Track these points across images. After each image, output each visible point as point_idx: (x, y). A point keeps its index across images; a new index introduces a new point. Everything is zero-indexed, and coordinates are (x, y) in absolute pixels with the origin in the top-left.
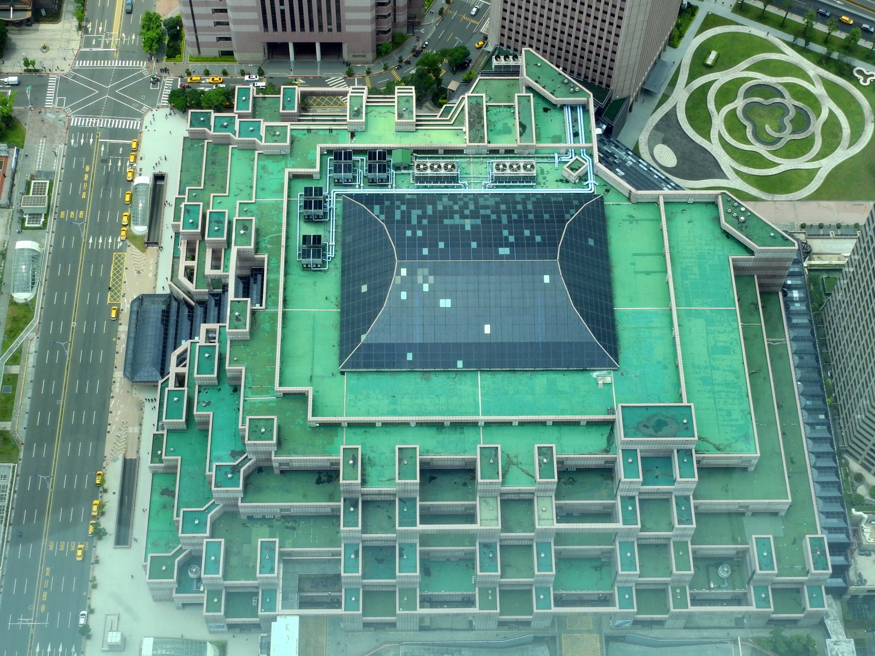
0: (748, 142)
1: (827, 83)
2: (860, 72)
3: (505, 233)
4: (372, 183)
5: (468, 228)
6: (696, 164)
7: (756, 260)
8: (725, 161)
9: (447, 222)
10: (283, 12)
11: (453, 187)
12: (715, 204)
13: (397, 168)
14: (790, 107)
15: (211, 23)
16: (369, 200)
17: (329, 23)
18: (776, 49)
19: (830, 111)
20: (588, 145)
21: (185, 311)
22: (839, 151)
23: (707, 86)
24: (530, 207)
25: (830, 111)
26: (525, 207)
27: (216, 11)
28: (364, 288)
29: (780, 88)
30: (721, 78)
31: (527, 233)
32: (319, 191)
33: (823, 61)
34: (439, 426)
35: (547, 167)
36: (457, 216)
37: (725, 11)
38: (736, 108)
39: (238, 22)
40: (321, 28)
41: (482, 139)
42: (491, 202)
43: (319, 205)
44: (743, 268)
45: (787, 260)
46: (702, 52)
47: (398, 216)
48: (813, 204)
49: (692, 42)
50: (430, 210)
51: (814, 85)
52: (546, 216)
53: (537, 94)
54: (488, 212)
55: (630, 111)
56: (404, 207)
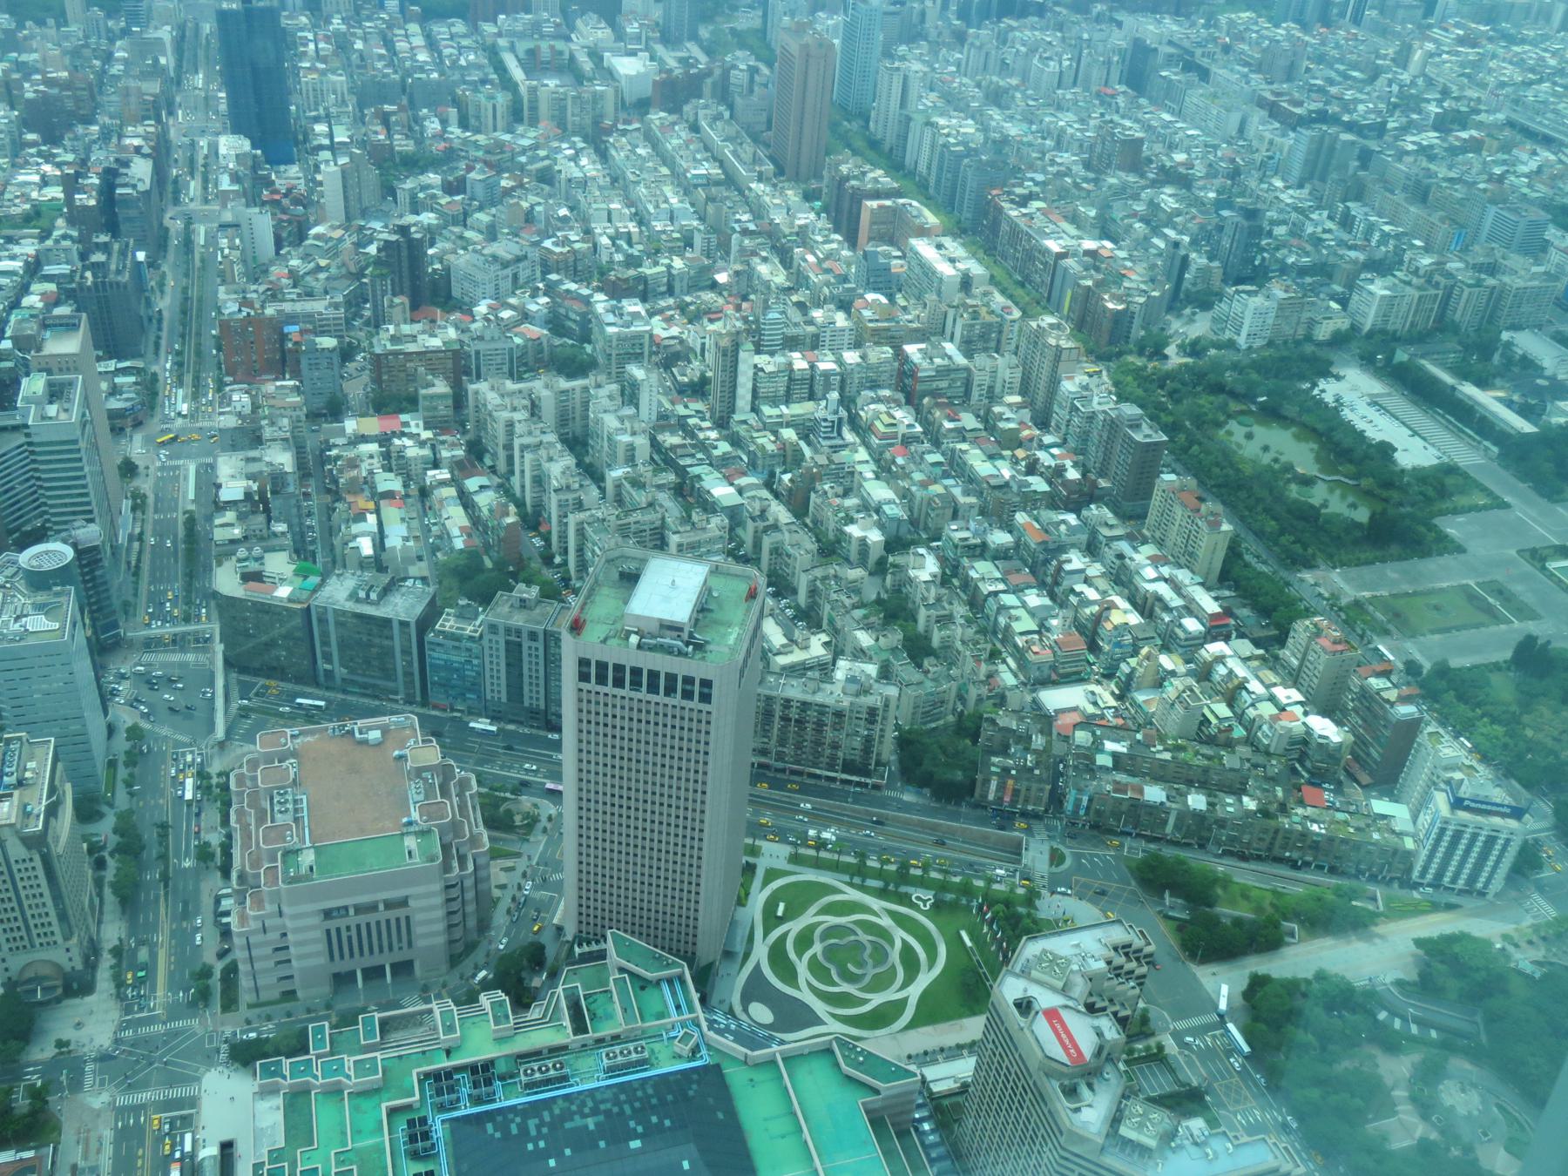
0: (834, 984)
1: (893, 915)
2: (918, 898)
3: (632, 1124)
4: (478, 1101)
5: (592, 1127)
6: (793, 1016)
8: (819, 1007)
9: (568, 1125)
10: (350, 938)
13: (502, 1078)
15: (272, 964)
16: (478, 1119)
17: (400, 940)
22: (920, 976)
23: (784, 937)
24: (650, 1091)
25: (903, 941)
30: (795, 927)
31: (654, 1119)
32: (423, 1121)
33: (882, 894)
35: (657, 1047)
36: (577, 1117)
37: (782, 864)
39: (300, 957)
40: (391, 949)
42: (609, 1094)
43: (426, 1136)
44: (875, 1110)
45: (911, 1093)
47: (514, 1130)
48: (912, 1033)
49: (759, 898)
50: (547, 1116)
52: (670, 1098)
53: (631, 974)
54: (608, 1106)
56: (518, 1120)
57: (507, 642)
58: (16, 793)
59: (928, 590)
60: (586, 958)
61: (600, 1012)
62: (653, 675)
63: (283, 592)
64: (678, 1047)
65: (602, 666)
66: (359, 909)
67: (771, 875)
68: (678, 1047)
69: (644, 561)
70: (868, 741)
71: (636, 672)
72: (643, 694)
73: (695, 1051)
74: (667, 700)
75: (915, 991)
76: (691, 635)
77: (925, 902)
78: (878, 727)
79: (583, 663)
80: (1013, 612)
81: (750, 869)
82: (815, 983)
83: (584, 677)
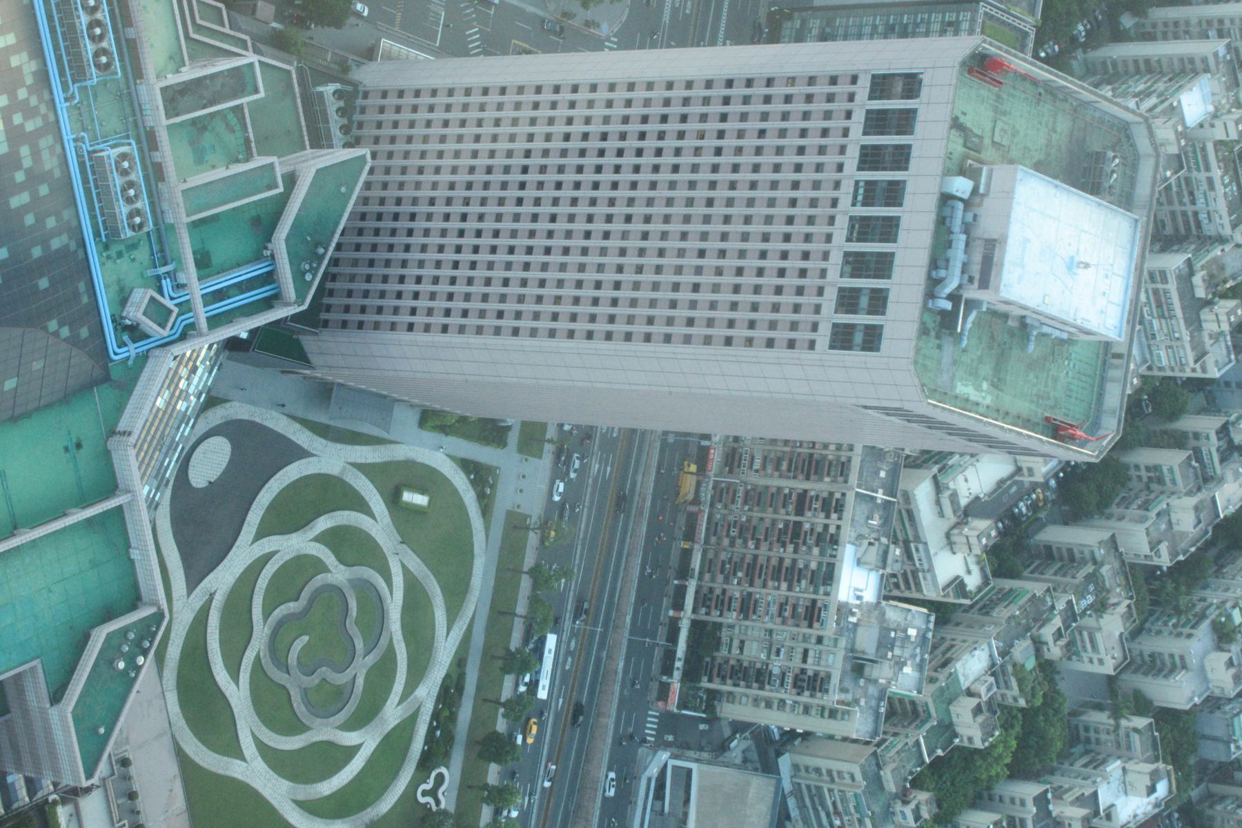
0: (266, 615)
1: (408, 725)
6: (204, 525)
7: (43, 711)
8: (223, 579)
11: (62, 73)
12: (135, 601)
14: (349, 672)
18: (452, 615)
19: (357, 748)
20: (203, 324)
22: (285, 785)
23: (361, 506)
25: (357, 748)
26: (56, 233)
29: (383, 642)
30: (379, 526)
35: (142, 254)
38: (329, 571)
41: (171, 111)
44: (21, 692)
45: (56, 771)
46: (425, 478)
48: (172, 768)
49: (437, 454)
51: (400, 703)
53: (284, 199)
54: (27, 163)
55: (283, 372)
59: (1080, 801)
60: (312, 104)
61: (208, 138)
62: (889, 229)
64: (141, 297)
65: (905, 121)
67: (479, 474)
68: (141, 297)
69: (1126, 201)
70: (761, 676)
71: (894, 194)
72: (847, 209)
73: (135, 332)
74: (836, 258)
75: (252, 771)
76: (971, 304)
77: (433, 793)
78: (789, 696)
79: (911, 84)
81: (492, 432)
83: (881, 85)
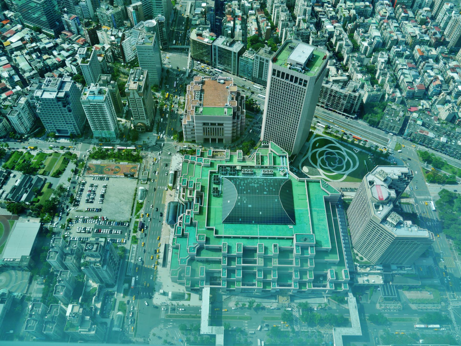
1: (347, 152)
3: (265, 188)
5: (256, 187)
9: (250, 185)
15: (190, 133)
21: (182, 206)
27: (192, 130)
28: (229, 202)
30: (320, 150)
31: (271, 188)
32: (218, 176)
34: (247, 238)
39: (197, 133)
41: (259, 164)
42: (262, 180)
46: (315, 143)
48: (344, 183)
50: (246, 182)
52: (276, 184)
57: (260, 62)
58: (138, 82)
59: (382, 64)
63: (206, 40)
65: (279, 72)
66: (212, 124)
70: (352, 105)
71: (288, 75)
72: (288, 81)
74: (295, 84)
79: (274, 70)
80: (406, 75)
82: (321, 165)
83: (274, 74)
